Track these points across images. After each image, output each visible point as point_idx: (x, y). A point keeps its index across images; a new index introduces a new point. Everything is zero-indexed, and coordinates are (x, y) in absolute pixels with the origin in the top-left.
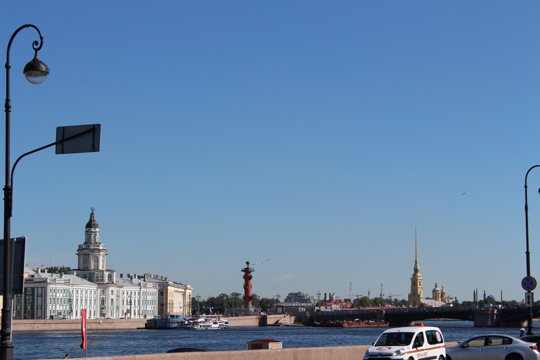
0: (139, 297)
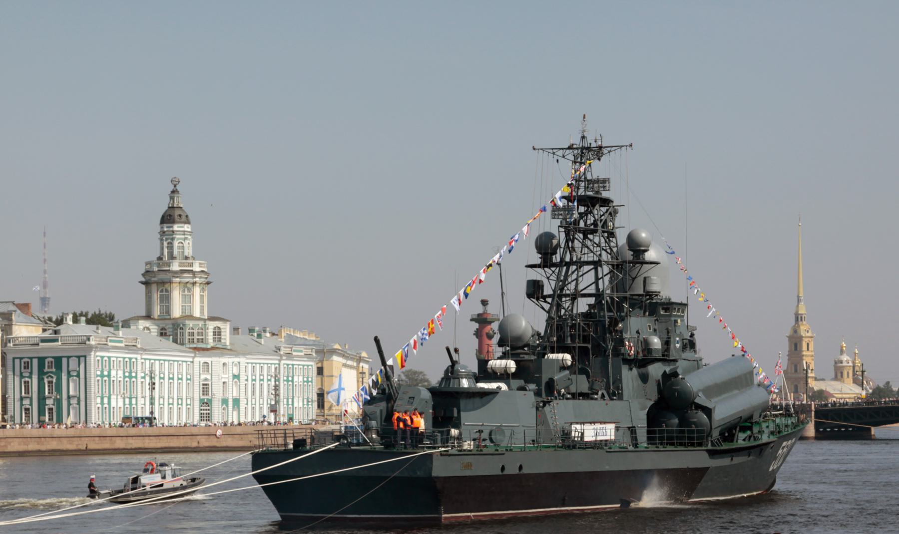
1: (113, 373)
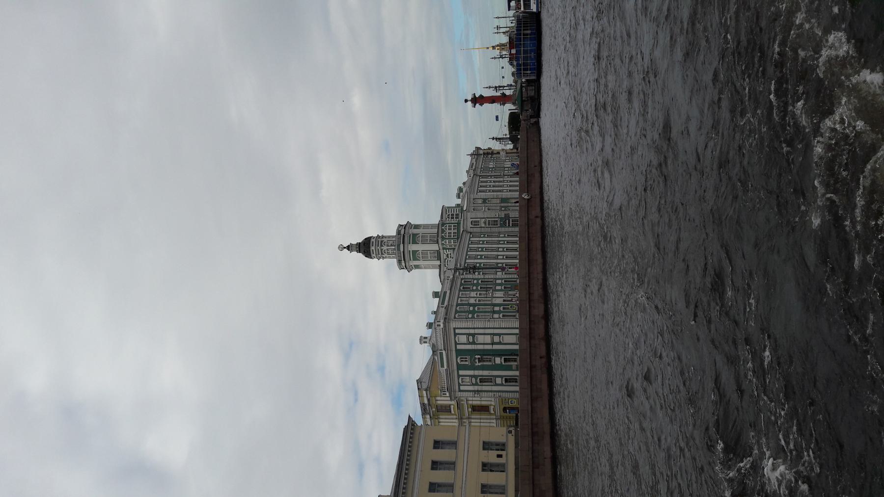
0: (489, 177)
1: (472, 301)
